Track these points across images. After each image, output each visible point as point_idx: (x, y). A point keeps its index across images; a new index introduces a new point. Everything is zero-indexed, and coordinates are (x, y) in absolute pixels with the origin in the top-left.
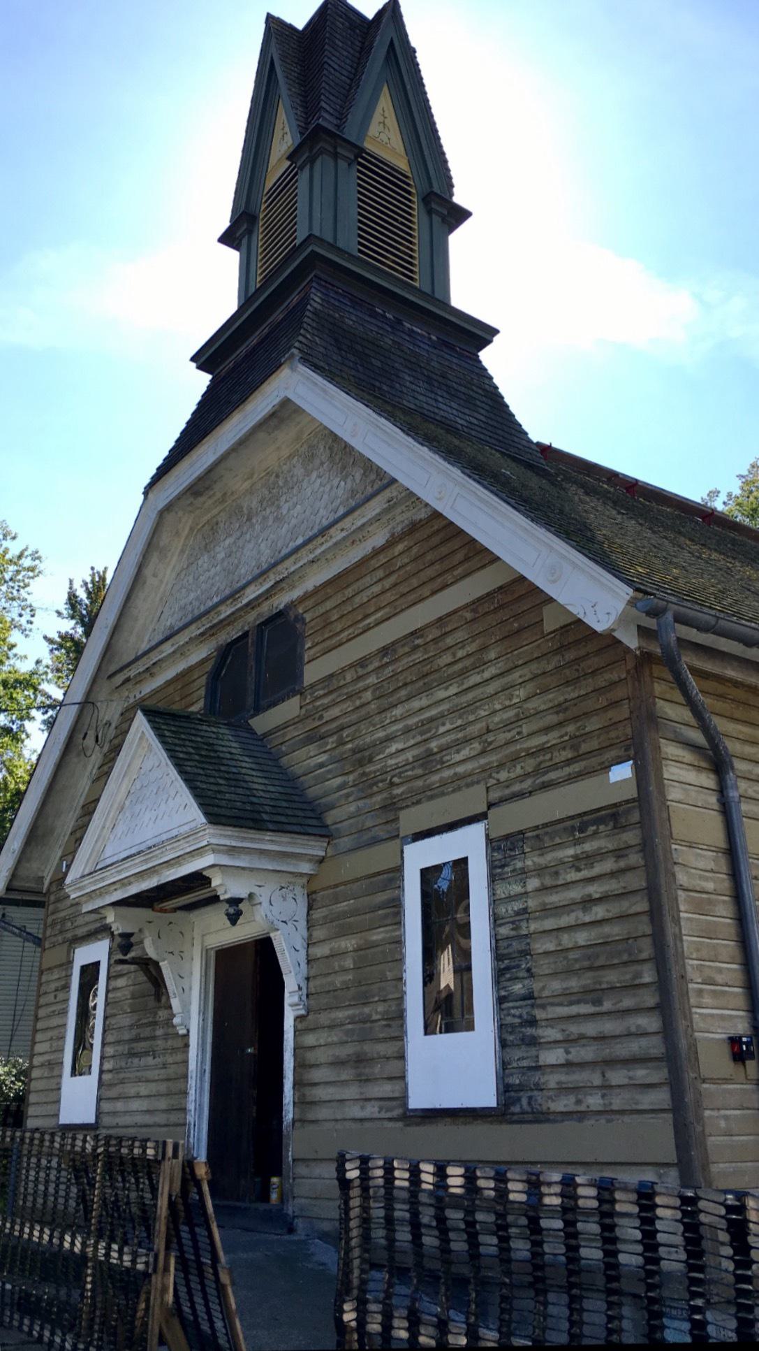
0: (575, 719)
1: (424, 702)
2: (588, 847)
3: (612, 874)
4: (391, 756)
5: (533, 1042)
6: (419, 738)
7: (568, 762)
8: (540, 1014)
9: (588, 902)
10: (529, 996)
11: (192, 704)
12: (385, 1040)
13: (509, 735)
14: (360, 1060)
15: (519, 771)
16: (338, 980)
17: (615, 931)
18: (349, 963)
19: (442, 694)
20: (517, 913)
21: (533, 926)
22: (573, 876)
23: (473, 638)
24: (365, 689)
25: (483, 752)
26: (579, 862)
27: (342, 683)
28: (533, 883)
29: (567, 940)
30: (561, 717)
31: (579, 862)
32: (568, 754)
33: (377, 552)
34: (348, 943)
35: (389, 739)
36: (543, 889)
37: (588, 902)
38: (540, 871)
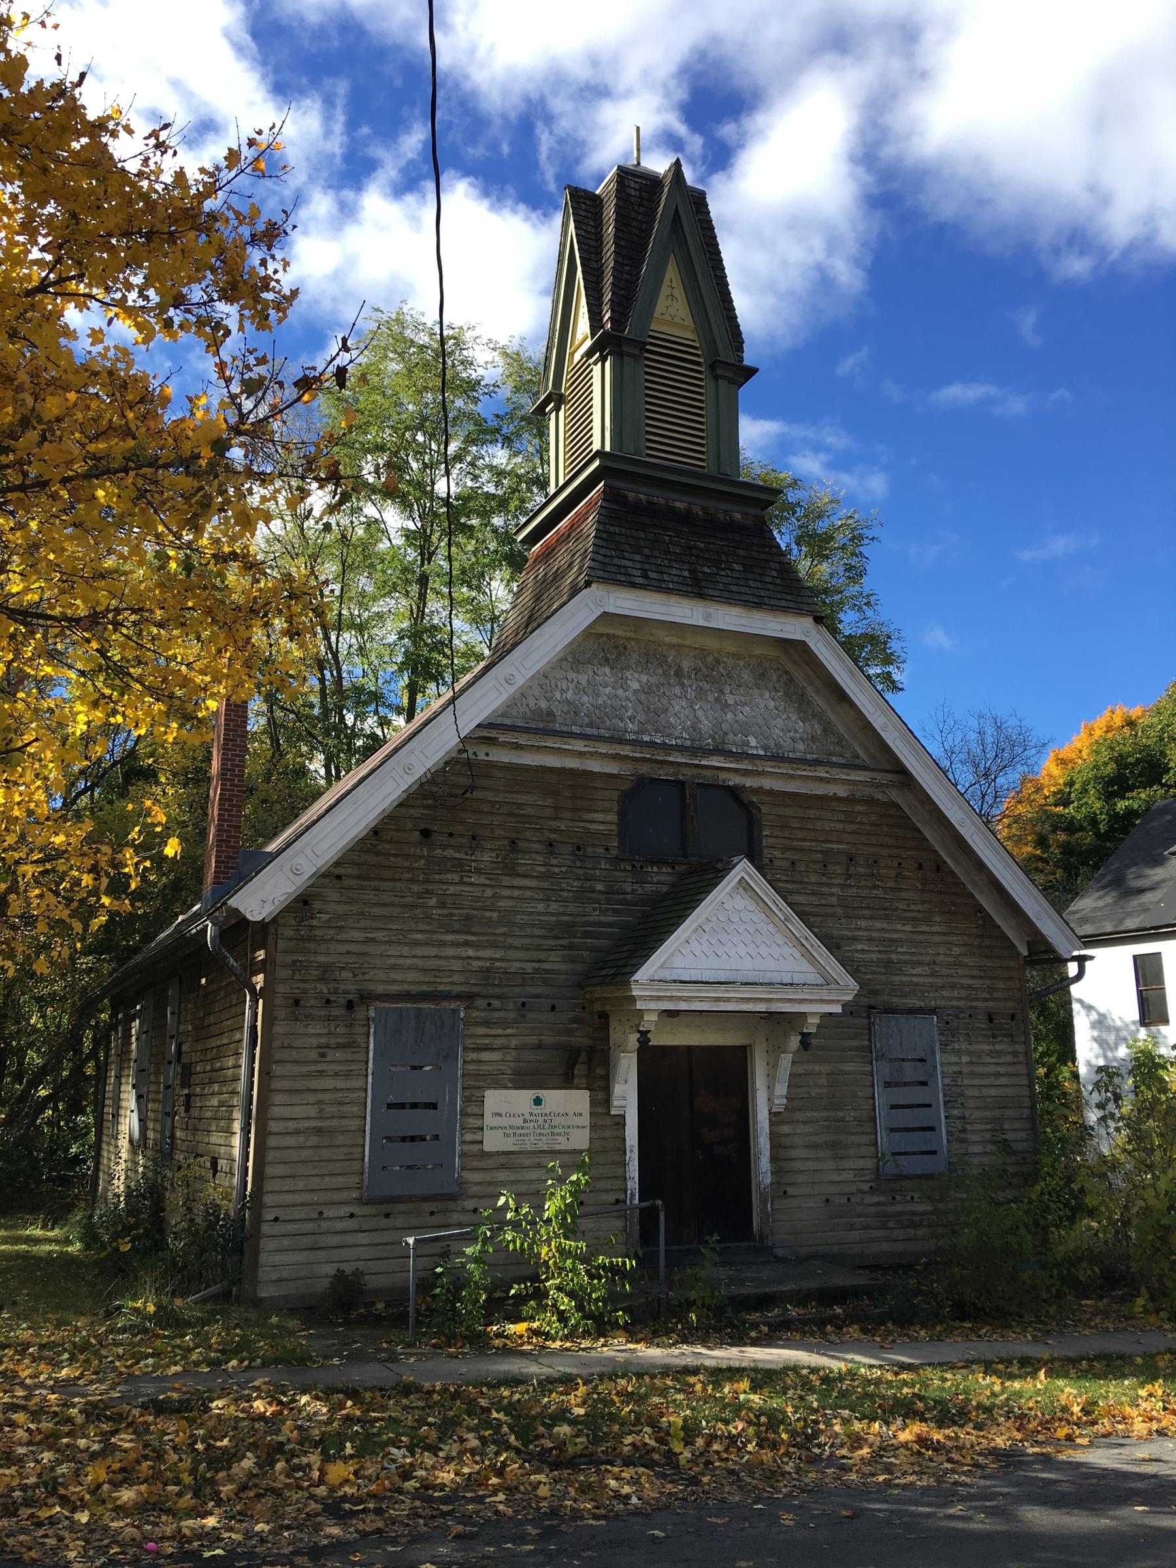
0: (991, 978)
1: (885, 926)
2: (998, 1047)
3: (1009, 1064)
4: (857, 951)
5: (965, 1141)
6: (881, 948)
7: (986, 1000)
8: (969, 1127)
9: (997, 1075)
10: (964, 1118)
11: (596, 811)
12: (857, 1133)
13: (950, 972)
14: (833, 1145)
15: (956, 994)
16: (814, 1092)
17: (1010, 1091)
18: (823, 1081)
19: (899, 927)
20: (955, 1073)
21: (965, 1082)
22: (988, 1060)
23: (923, 902)
24: (831, 895)
25: (931, 975)
26: (990, 1053)
27: (806, 880)
28: (965, 1059)
29: (985, 1092)
30: (982, 974)
31: (990, 1053)
32: (985, 995)
33: (836, 798)
34: (825, 1068)
35: (855, 939)
36: (972, 1063)
37: (997, 1075)
38: (969, 1053)
